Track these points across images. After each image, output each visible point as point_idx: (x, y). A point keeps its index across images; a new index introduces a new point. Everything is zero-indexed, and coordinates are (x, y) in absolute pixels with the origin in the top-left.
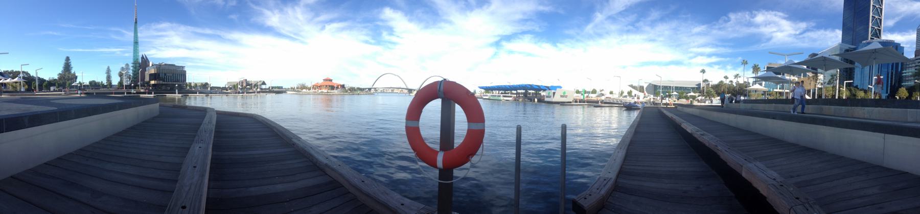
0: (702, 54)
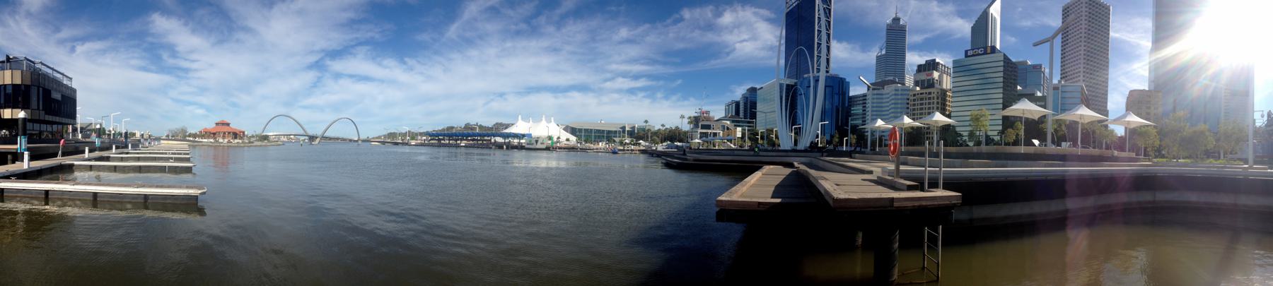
0: (624, 75)
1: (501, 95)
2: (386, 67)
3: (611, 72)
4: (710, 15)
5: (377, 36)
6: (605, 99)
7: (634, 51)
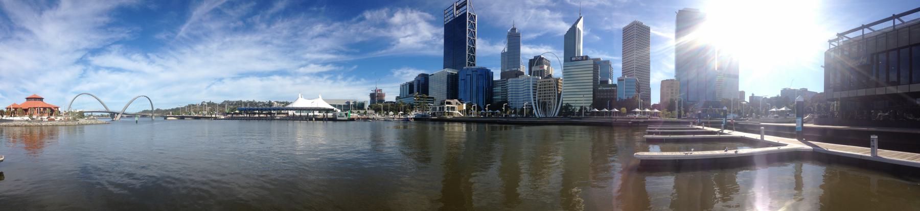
0: (315, 62)
1: (221, 80)
2: (135, 61)
3: (306, 60)
4: (385, 15)
6: (298, 81)
7: (326, 43)
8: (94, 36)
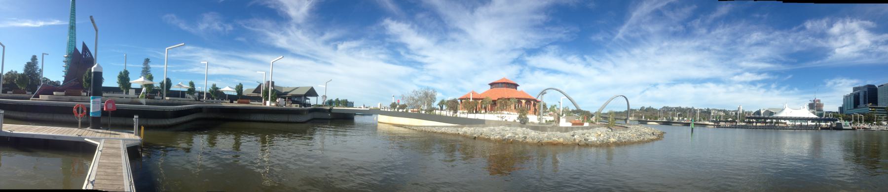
0: (750, 70)
2: (571, 63)
3: (742, 68)
4: (825, 25)
5: (563, 36)
6: (732, 89)
7: (764, 52)
8: (531, 35)
